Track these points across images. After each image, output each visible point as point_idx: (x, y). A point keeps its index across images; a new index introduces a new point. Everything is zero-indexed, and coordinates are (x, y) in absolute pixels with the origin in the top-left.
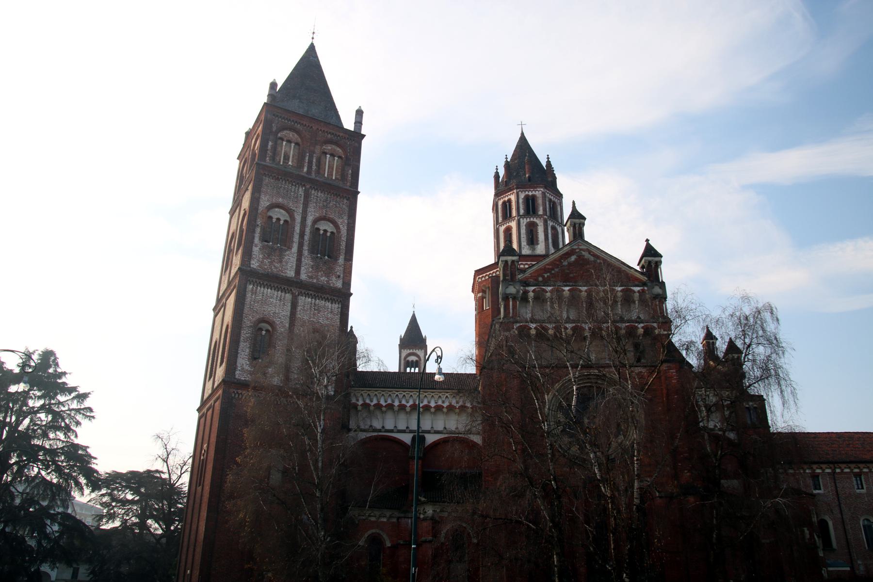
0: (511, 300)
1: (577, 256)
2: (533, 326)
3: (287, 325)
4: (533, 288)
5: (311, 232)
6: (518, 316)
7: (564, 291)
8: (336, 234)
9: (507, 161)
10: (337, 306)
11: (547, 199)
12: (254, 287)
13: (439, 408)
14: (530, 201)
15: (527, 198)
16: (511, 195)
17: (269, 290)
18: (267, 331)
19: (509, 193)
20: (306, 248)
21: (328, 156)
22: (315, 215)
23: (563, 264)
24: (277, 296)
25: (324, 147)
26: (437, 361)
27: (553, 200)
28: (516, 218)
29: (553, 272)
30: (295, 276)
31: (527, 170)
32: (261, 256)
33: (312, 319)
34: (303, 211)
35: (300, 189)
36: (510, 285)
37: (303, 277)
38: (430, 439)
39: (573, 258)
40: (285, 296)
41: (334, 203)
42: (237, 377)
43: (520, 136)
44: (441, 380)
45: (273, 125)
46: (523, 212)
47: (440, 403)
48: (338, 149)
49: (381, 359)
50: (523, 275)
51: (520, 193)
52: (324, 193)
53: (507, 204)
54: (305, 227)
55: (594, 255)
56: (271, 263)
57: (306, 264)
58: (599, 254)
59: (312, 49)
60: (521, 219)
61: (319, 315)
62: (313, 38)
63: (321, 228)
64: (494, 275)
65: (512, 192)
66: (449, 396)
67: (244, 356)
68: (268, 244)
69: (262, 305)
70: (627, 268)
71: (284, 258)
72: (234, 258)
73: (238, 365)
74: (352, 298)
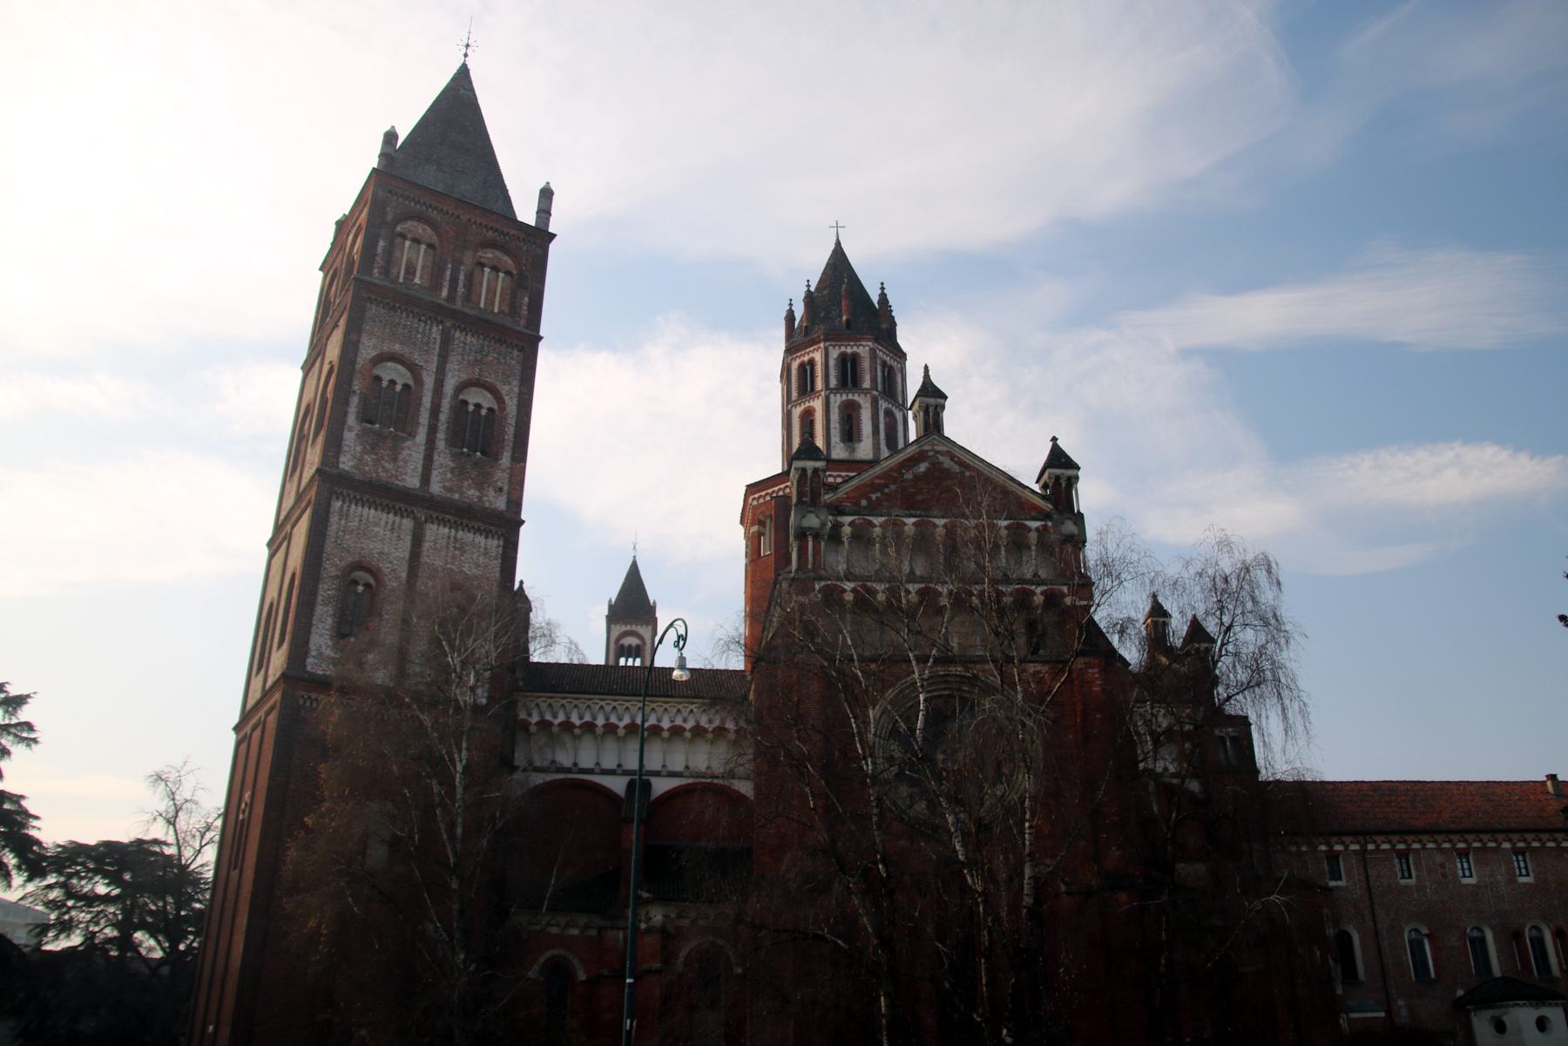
0: (810, 539)
1: (930, 464)
2: (849, 586)
3: (404, 575)
4: (850, 519)
5: (451, 407)
6: (822, 567)
7: (905, 524)
8: (497, 413)
9: (809, 291)
10: (495, 542)
11: (879, 362)
12: (345, 506)
13: (676, 731)
14: (849, 364)
16: (815, 352)
17: (372, 511)
18: (367, 585)
19: (812, 349)
20: (441, 435)
21: (487, 270)
22: (460, 377)
23: (905, 477)
24: (387, 523)
25: (480, 254)
26: (677, 644)
27: (889, 363)
28: (823, 393)
29: (886, 491)
30: (421, 486)
31: (844, 308)
32: (359, 449)
33: (449, 566)
35: (435, 329)
36: (811, 512)
37: (436, 488)
38: (661, 786)
39: (923, 467)
40: (400, 523)
41: (496, 355)
42: (309, 668)
43: (833, 246)
44: (684, 679)
45: (388, 209)
46: (835, 383)
47: (679, 722)
48: (506, 258)
49: (575, 639)
50: (832, 495)
51: (831, 348)
52: (479, 337)
53: (808, 368)
54: (441, 398)
55: (961, 463)
56: (378, 461)
57: (441, 465)
58: (968, 462)
59: (463, 74)
60: (832, 396)
61: (463, 558)
62: (466, 55)
63: (469, 401)
64: (781, 493)
65: (816, 347)
66: (695, 710)
67: (324, 631)
68: (372, 426)
69: (359, 539)
70: (1017, 487)
71: (400, 453)
72: (309, 450)
73: (312, 646)
74: (523, 529)
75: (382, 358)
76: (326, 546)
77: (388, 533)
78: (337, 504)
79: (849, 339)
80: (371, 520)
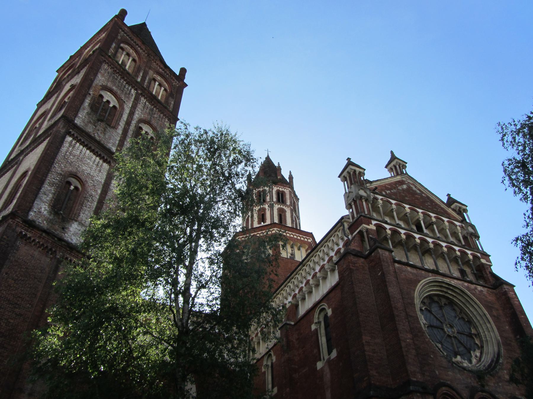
0: (363, 201)
3: (99, 191)
15: (278, 192)
21: (157, 83)
23: (399, 188)
29: (392, 191)
34: (132, 106)
40: (102, 164)
42: (30, 217)
48: (165, 83)
63: (144, 129)
69: (78, 161)
75: (105, 88)
76: (58, 156)
77: (95, 166)
78: (69, 139)
79: (281, 185)
80: (87, 155)
